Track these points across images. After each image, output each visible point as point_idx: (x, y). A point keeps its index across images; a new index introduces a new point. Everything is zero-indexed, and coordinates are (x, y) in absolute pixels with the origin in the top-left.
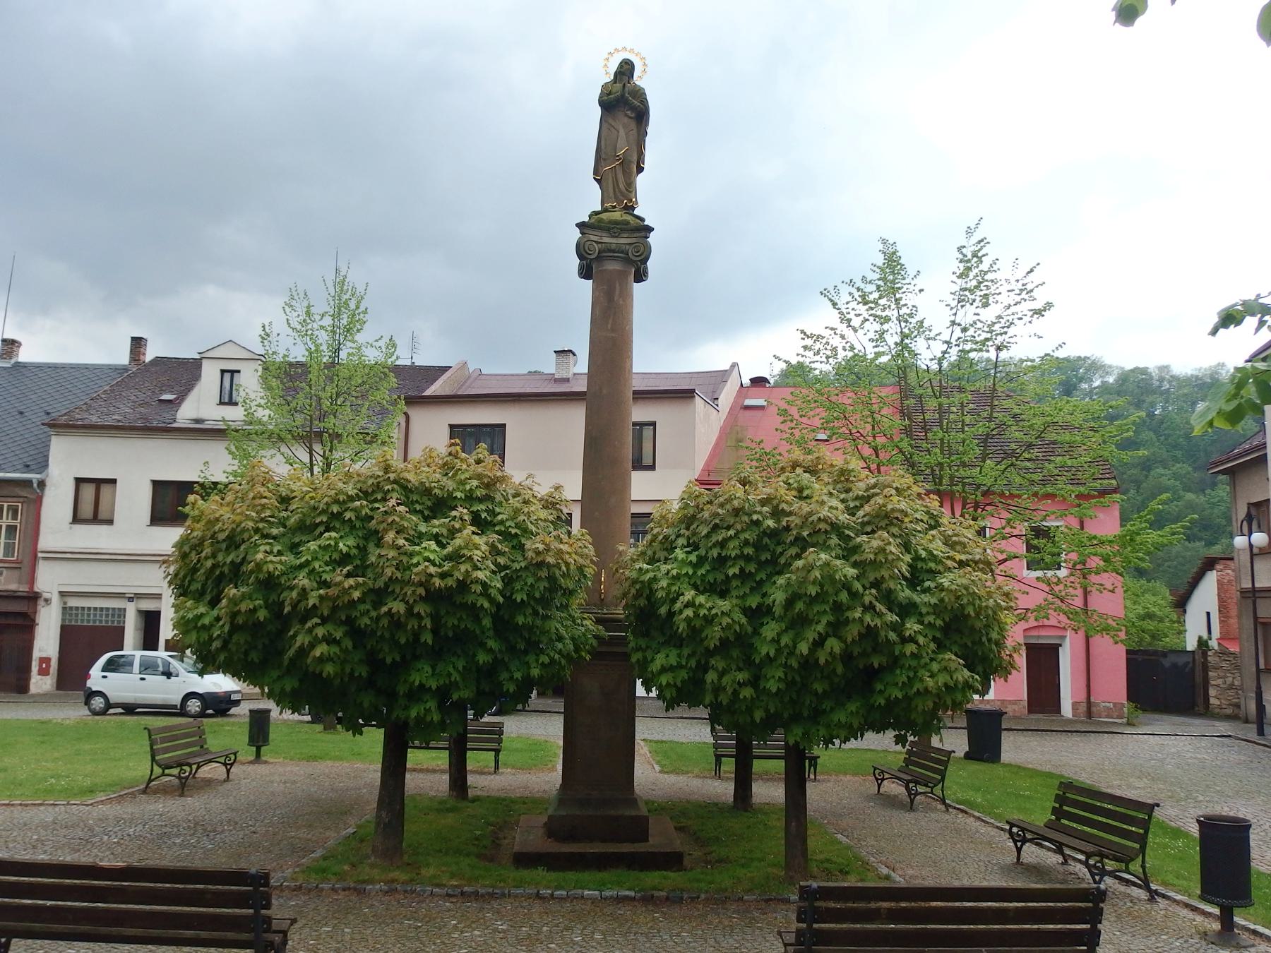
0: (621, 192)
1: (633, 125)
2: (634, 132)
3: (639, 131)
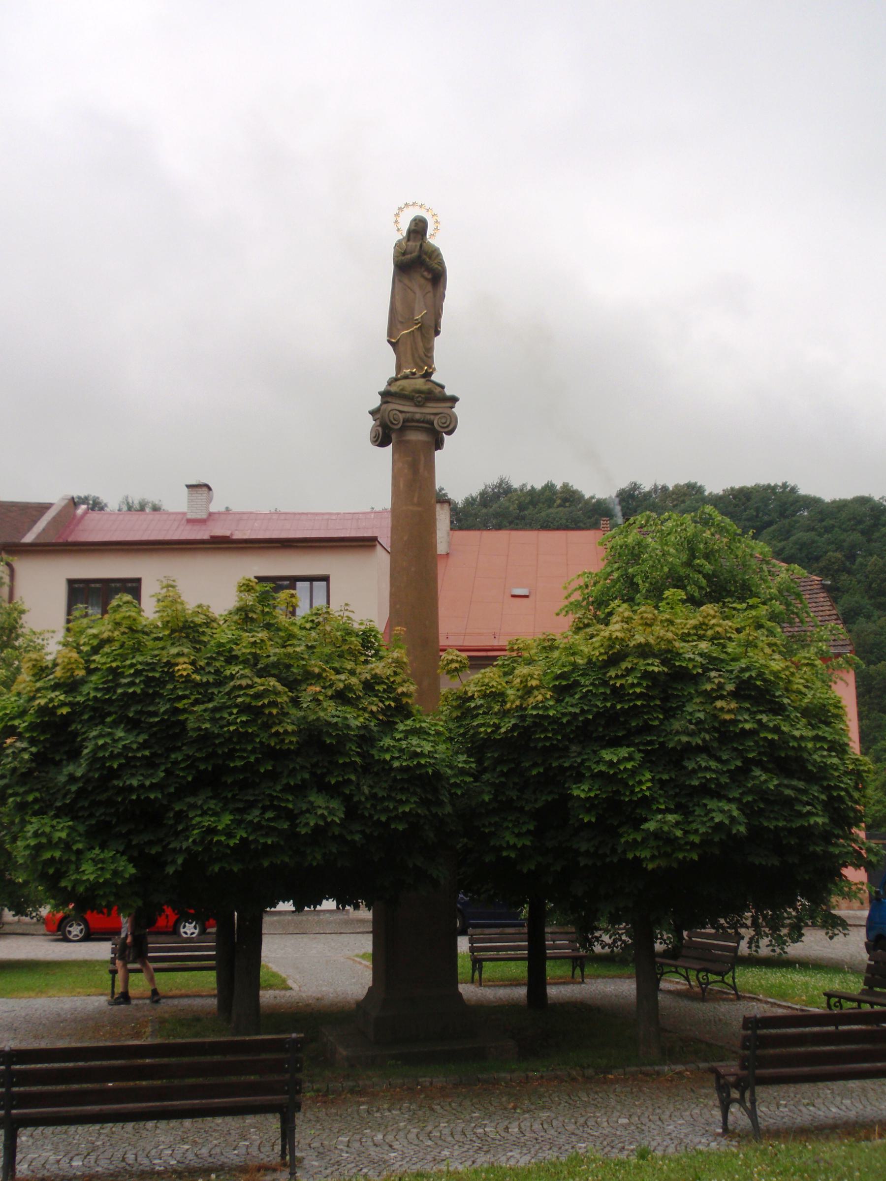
0: (421, 358)
1: (429, 287)
2: (430, 295)
3: (435, 296)
